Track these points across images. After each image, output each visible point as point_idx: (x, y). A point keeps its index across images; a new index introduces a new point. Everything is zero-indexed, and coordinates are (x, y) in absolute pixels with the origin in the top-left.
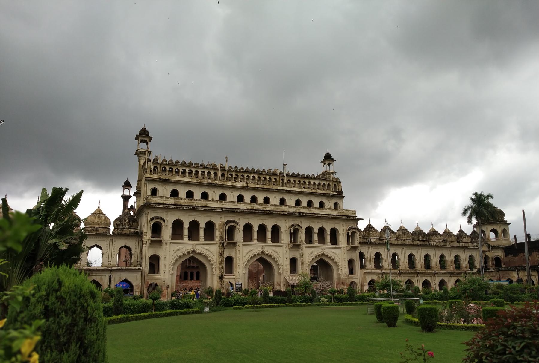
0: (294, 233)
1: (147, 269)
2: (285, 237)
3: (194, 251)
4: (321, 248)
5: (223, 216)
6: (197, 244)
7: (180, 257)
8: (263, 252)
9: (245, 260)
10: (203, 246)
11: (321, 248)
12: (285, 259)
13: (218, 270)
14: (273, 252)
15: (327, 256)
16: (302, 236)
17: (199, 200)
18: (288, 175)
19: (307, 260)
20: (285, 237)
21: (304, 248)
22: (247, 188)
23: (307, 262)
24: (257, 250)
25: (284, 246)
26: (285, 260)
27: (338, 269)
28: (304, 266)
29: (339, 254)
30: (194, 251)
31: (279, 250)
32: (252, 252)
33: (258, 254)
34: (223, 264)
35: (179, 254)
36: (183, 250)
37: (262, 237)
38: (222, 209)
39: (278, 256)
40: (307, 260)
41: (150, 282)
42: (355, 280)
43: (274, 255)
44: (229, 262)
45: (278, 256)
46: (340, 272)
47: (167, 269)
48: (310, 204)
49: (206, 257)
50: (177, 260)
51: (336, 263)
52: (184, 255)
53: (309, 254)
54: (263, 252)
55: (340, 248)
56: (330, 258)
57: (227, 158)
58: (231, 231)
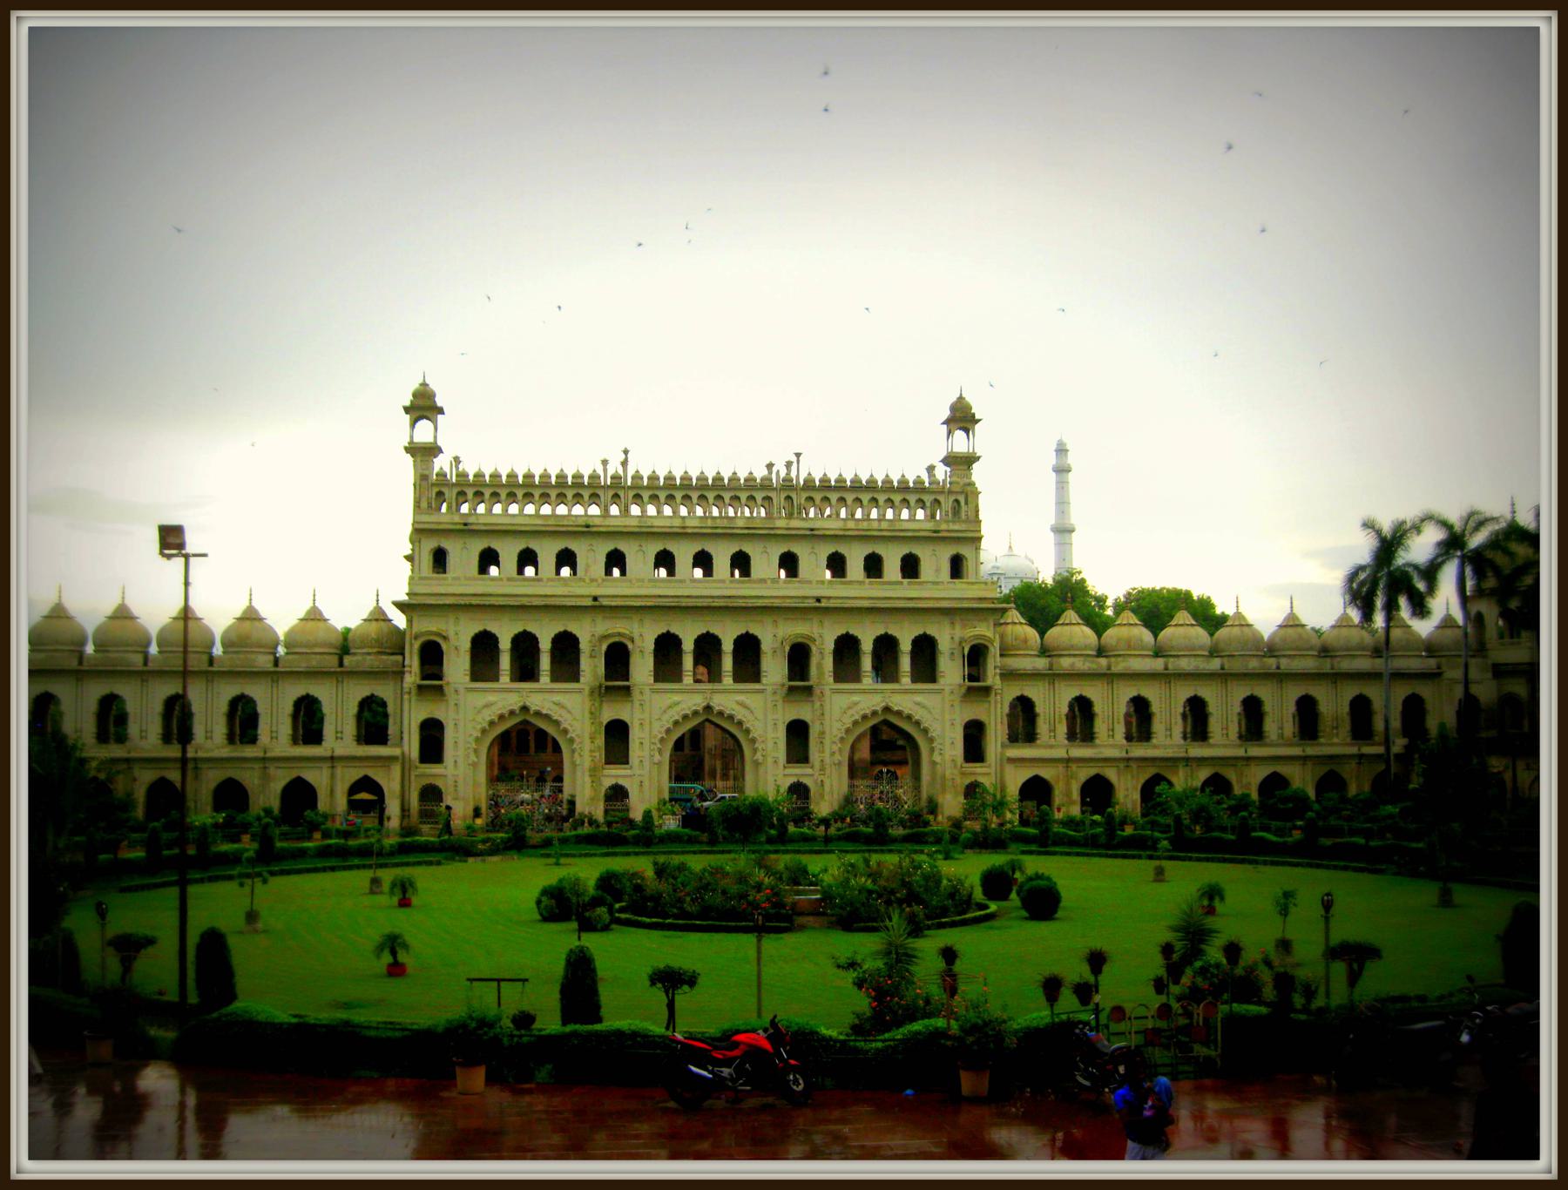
0: (799, 657)
1: (415, 752)
2: (774, 669)
3: (525, 709)
5: (599, 619)
6: (532, 691)
7: (492, 723)
9: (659, 729)
10: (547, 696)
12: (770, 723)
13: (586, 754)
15: (899, 713)
16: (822, 662)
18: (809, 485)
19: (838, 725)
20: (774, 669)
21: (827, 693)
26: (770, 728)
27: (932, 750)
28: (827, 742)
29: (936, 711)
30: (525, 709)
31: (755, 701)
32: (677, 708)
33: (696, 713)
34: (601, 741)
35: (489, 715)
36: (500, 705)
38: (595, 599)
39: (750, 717)
41: (426, 781)
42: (981, 779)
43: (740, 714)
44: (617, 734)
46: (937, 757)
47: (461, 753)
48: (874, 566)
49: (557, 723)
50: (484, 731)
51: (926, 731)
52: (501, 717)
53: (843, 708)
54: (708, 708)
55: (941, 691)
56: (909, 717)
58: (618, 658)
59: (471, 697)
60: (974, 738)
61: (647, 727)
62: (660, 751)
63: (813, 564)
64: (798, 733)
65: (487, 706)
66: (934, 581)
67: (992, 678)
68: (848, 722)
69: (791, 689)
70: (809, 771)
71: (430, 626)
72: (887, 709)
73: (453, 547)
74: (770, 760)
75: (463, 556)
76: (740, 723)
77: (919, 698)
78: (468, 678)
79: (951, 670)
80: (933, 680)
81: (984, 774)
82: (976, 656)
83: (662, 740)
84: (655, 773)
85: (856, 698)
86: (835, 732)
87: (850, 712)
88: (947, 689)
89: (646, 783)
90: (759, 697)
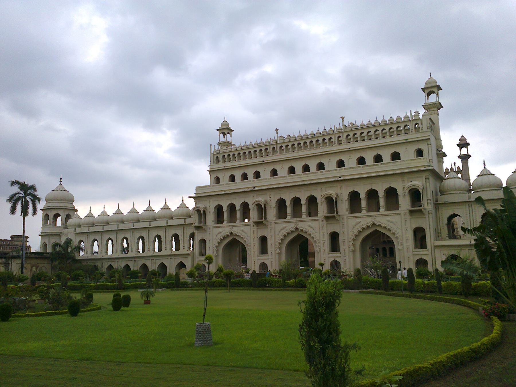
4: (370, 216)
8: (297, 229)
11: (370, 216)
12: (321, 234)
14: (309, 228)
15: (380, 226)
17: (315, 173)
19: (351, 233)
20: (322, 209)
22: (263, 164)
23: (351, 236)
24: (291, 227)
25: (320, 220)
29: (398, 225)
31: (315, 224)
32: (285, 229)
37: (232, 218)
39: (313, 231)
40: (351, 233)
43: (310, 230)
45: (313, 231)
51: (394, 234)
55: (400, 214)
56: (385, 228)
57: (277, 130)
59: (215, 230)
60: (420, 237)
61: (273, 238)
62: (280, 248)
63: (351, 161)
64: (334, 237)
65: (219, 233)
66: (409, 160)
67: (427, 205)
68: (356, 231)
69: (411, 212)
70: (339, 255)
71: (201, 206)
72: (374, 224)
73: (220, 175)
74: (322, 250)
75: (224, 178)
76: (310, 234)
77: (389, 218)
78: (215, 223)
79: (405, 202)
80: (398, 209)
81: (424, 254)
82: (416, 195)
83: (280, 244)
84: (277, 257)
85: (358, 220)
86: (351, 236)
87: (357, 227)
88: (403, 213)
89: (274, 262)
90: (317, 222)
